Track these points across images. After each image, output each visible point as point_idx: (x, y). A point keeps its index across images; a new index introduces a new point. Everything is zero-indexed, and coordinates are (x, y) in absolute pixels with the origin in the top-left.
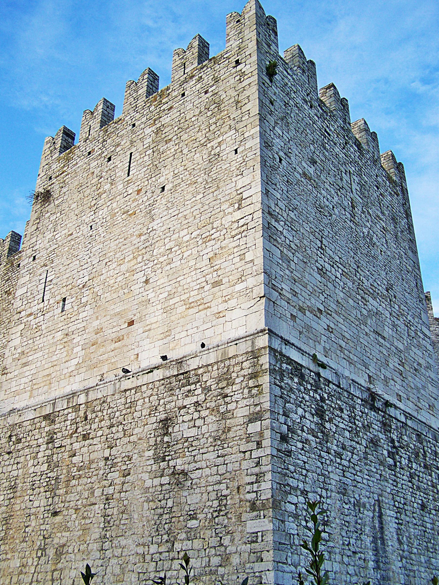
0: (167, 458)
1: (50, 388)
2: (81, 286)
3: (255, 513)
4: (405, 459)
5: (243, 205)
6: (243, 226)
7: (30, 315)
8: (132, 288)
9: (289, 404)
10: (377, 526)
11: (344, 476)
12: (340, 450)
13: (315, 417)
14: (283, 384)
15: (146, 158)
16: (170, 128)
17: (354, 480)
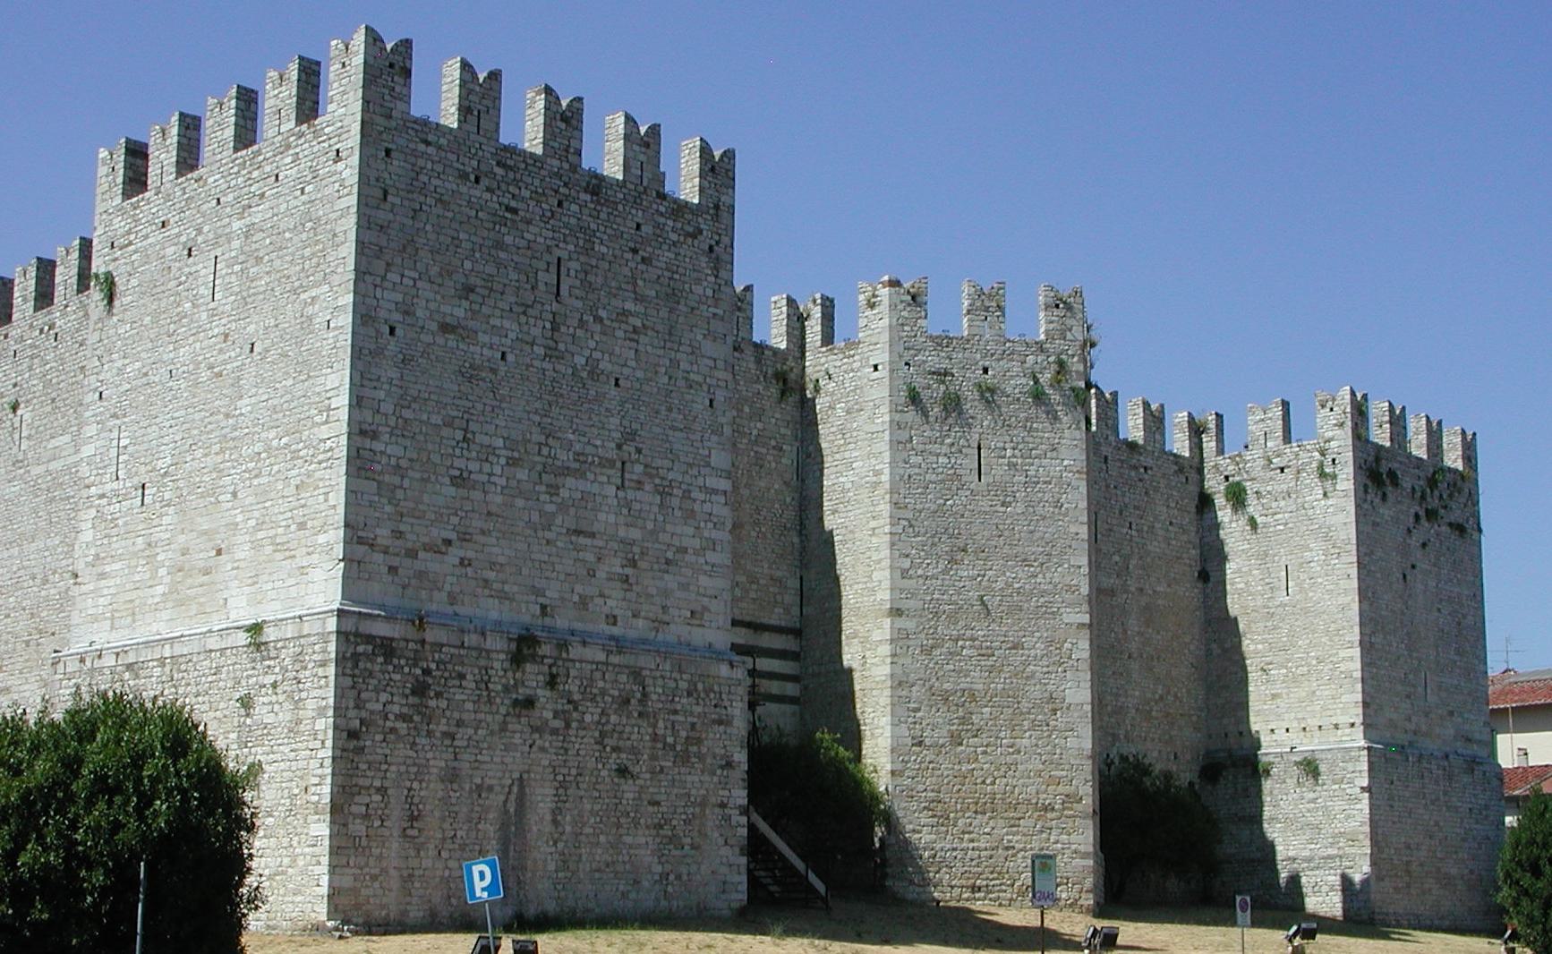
0: (250, 744)
1: (134, 621)
2: (162, 471)
3: (317, 817)
4: (592, 714)
5: (331, 419)
6: (328, 451)
7: (102, 496)
8: (220, 498)
9: (366, 693)
10: (512, 810)
11: (456, 759)
12: (453, 729)
13: (410, 698)
14: (357, 672)
15: (233, 278)
16: (262, 235)
17: (476, 761)
